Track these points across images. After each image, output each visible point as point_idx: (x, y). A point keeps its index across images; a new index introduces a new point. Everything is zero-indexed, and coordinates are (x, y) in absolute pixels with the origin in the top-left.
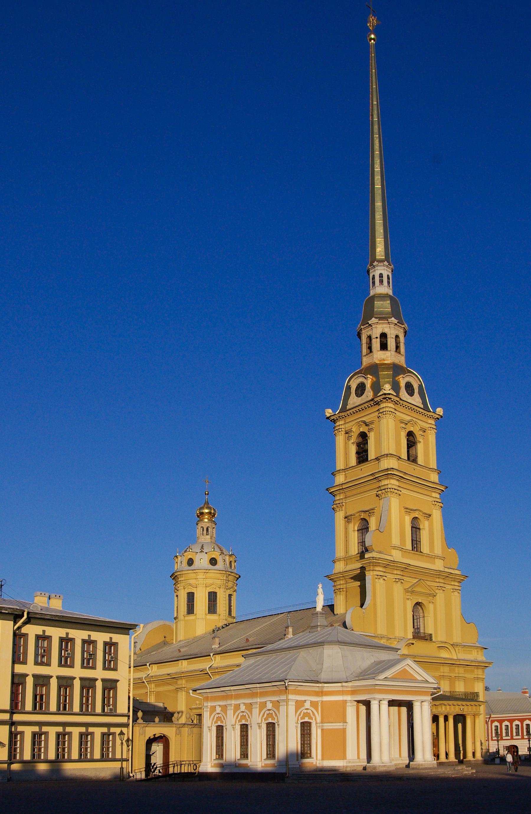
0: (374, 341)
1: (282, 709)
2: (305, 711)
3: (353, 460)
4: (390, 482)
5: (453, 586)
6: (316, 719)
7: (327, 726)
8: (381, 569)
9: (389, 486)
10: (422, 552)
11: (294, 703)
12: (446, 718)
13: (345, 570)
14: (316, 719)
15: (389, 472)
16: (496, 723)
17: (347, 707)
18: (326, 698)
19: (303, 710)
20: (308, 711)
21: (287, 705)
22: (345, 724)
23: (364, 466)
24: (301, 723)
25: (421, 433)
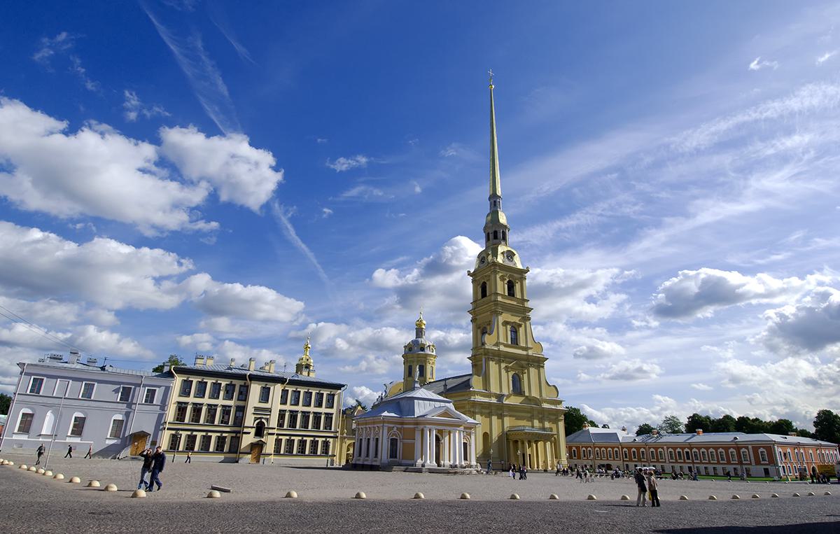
1: (381, 431)
7: (406, 441)
16: (597, 449)
18: (405, 426)
23: (485, 299)
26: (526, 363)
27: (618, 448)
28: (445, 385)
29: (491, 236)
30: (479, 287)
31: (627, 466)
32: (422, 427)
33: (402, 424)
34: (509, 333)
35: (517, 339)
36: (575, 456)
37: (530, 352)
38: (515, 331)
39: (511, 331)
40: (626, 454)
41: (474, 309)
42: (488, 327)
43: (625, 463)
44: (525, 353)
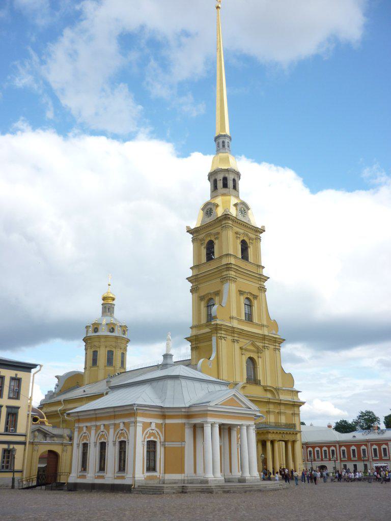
1: (132, 429)
2: (151, 431)
3: (204, 259)
6: (160, 438)
7: (168, 444)
8: (223, 332)
10: (251, 321)
11: (141, 425)
12: (272, 442)
13: (199, 333)
14: (160, 438)
16: (310, 449)
17: (186, 429)
18: (168, 421)
20: (154, 431)
21: (136, 426)
22: (183, 443)
23: (211, 262)
24: (149, 442)
25: (251, 241)
26: (262, 345)
27: (335, 446)
29: (220, 184)
30: (203, 247)
31: (345, 466)
34: (243, 305)
37: (266, 332)
38: (250, 305)
39: (245, 304)
40: (344, 453)
42: (217, 299)
43: (343, 463)
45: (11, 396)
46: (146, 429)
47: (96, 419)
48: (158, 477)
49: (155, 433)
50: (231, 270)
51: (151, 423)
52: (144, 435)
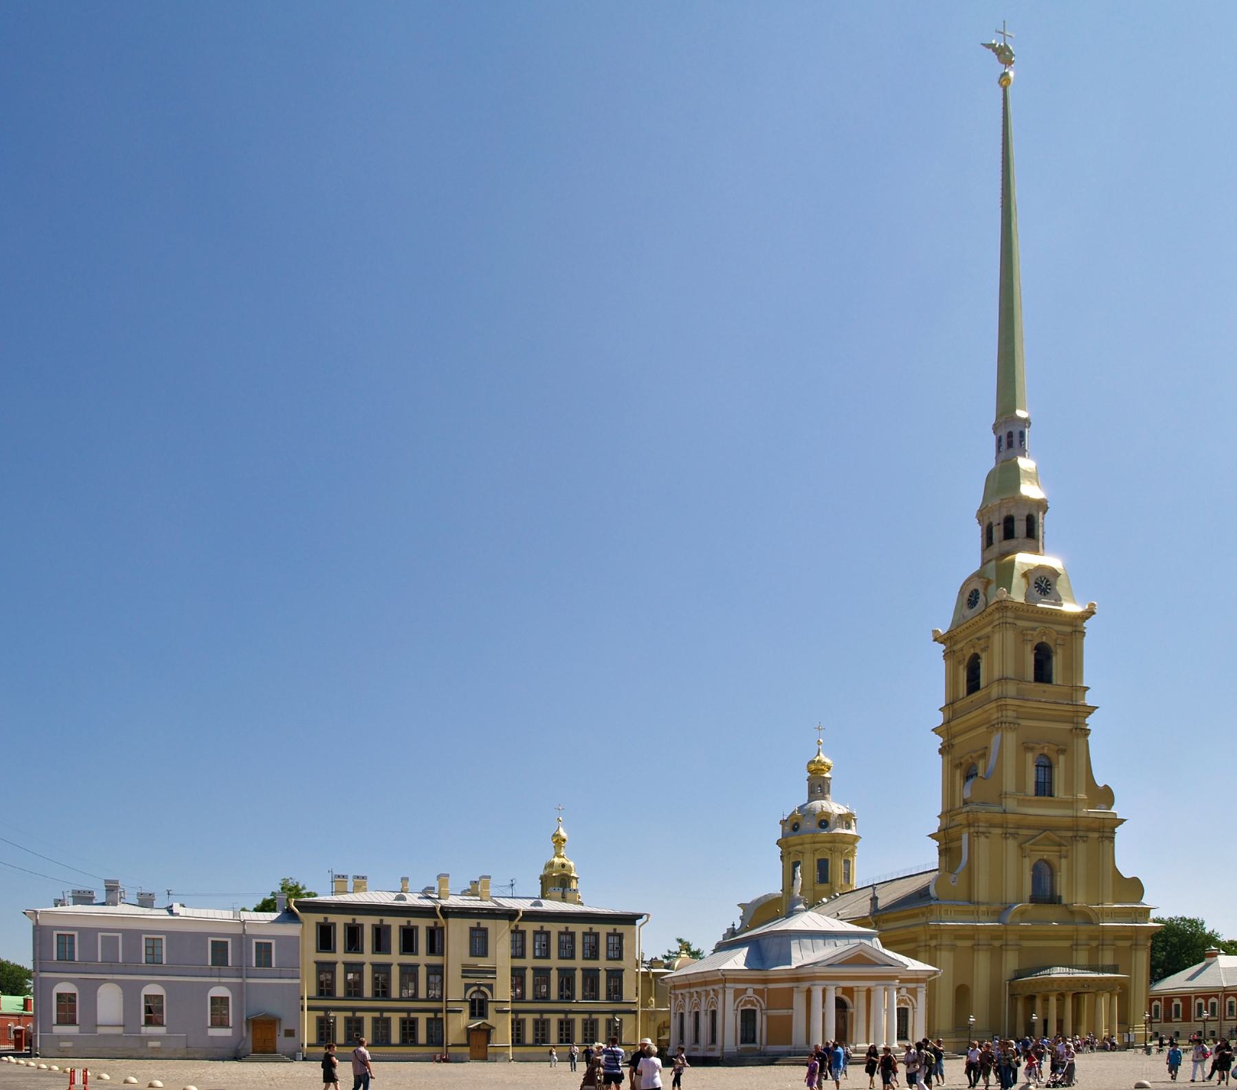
0: (995, 529)
1: (721, 997)
2: (747, 999)
4: (1002, 714)
5: (1101, 834)
6: (761, 1006)
9: (1000, 720)
10: (1051, 795)
11: (733, 992)
14: (761, 1006)
15: (1002, 703)
18: (771, 986)
19: (745, 998)
22: (790, 1011)
23: (976, 696)
24: (742, 1010)
28: (874, 899)
30: (961, 667)
32: (805, 985)
33: (765, 981)
35: (1051, 783)
36: (1177, 1015)
38: (1046, 767)
41: (947, 722)
44: (1069, 812)
45: (611, 954)
46: (742, 995)
47: (690, 985)
48: (758, 1048)
49: (753, 1001)
50: (1006, 710)
51: (746, 989)
52: (736, 1003)
